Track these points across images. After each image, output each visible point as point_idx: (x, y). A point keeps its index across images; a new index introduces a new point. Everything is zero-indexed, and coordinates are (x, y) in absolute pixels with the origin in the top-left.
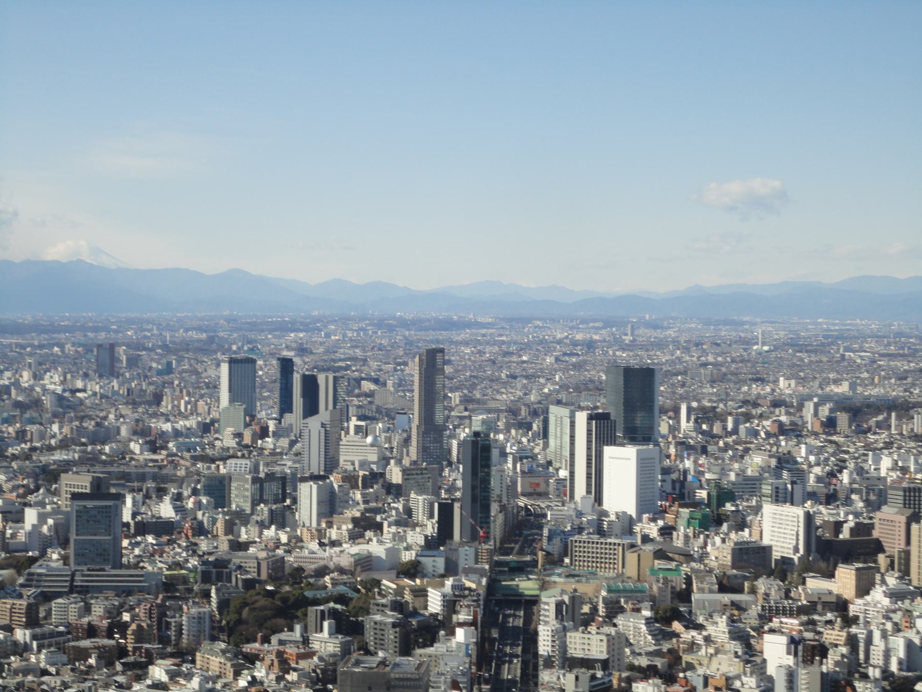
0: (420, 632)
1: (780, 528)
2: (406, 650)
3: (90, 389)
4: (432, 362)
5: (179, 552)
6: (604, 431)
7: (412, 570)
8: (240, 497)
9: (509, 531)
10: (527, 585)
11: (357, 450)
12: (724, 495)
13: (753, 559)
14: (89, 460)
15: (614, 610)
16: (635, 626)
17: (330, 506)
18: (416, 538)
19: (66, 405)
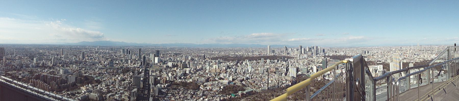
0: (140, 73)
1: (170, 64)
2: (138, 74)
3: (110, 52)
4: (140, 50)
5: (118, 66)
6: (155, 56)
7: (139, 68)
8: (123, 61)
9: (146, 64)
10: (148, 69)
11: (133, 57)
12: (165, 61)
13: (168, 67)
14: (110, 58)
15: (156, 71)
16: (158, 73)
17: (131, 62)
18: (139, 65)
19: (108, 53)
